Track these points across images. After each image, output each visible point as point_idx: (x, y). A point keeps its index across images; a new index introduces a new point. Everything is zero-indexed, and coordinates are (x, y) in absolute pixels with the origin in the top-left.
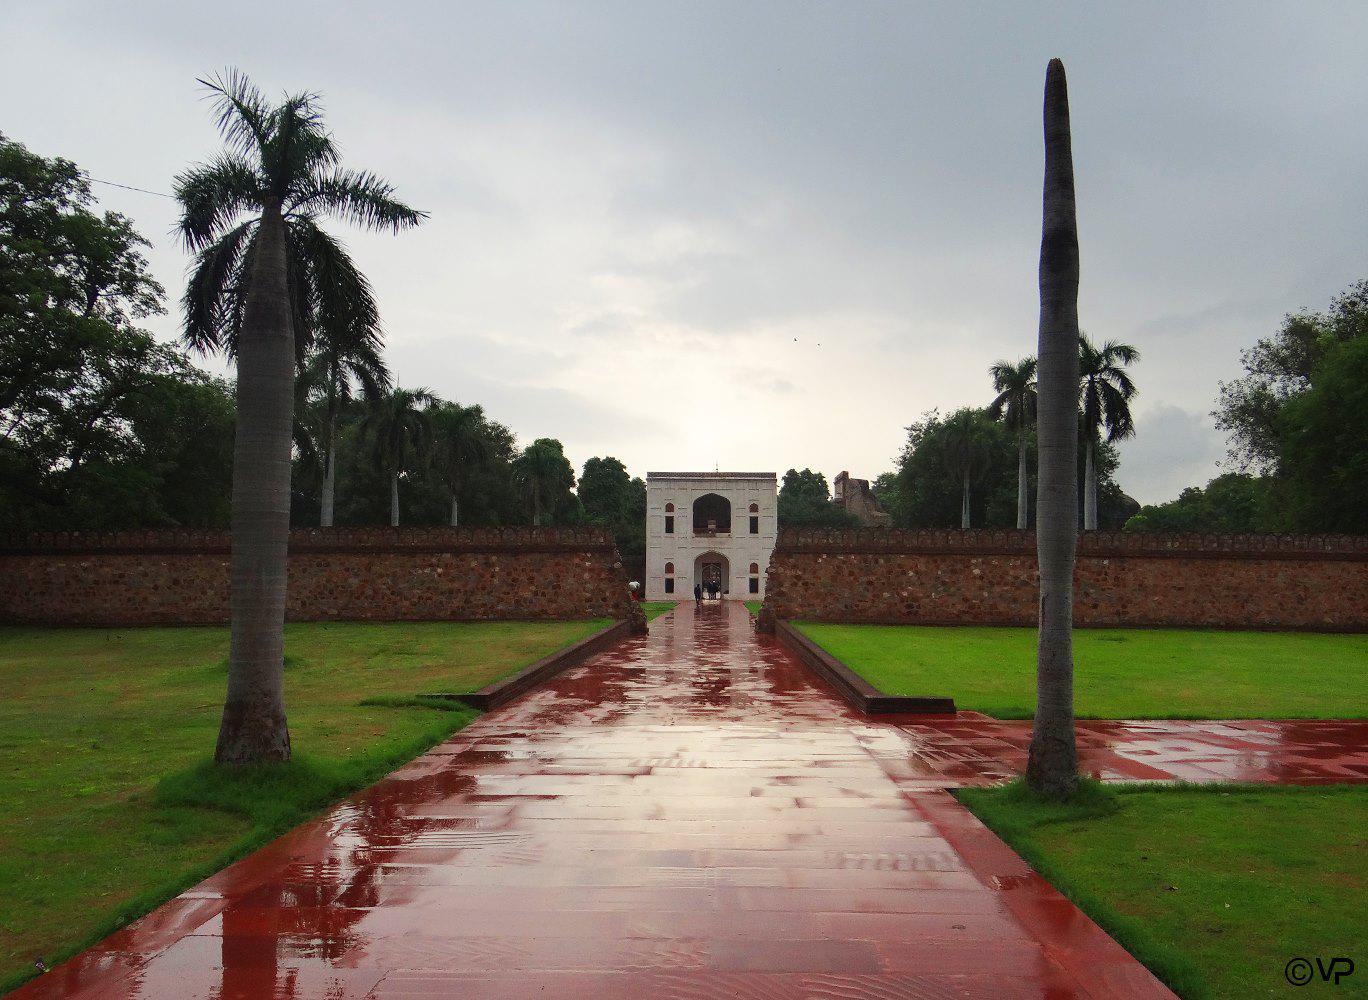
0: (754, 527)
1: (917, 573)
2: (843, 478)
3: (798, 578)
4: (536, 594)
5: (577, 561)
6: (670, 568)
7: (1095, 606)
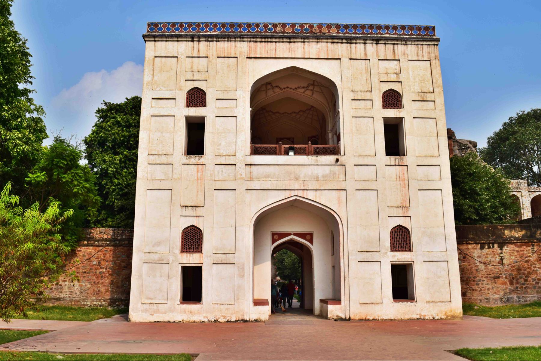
0: (394, 139)
6: (192, 239)
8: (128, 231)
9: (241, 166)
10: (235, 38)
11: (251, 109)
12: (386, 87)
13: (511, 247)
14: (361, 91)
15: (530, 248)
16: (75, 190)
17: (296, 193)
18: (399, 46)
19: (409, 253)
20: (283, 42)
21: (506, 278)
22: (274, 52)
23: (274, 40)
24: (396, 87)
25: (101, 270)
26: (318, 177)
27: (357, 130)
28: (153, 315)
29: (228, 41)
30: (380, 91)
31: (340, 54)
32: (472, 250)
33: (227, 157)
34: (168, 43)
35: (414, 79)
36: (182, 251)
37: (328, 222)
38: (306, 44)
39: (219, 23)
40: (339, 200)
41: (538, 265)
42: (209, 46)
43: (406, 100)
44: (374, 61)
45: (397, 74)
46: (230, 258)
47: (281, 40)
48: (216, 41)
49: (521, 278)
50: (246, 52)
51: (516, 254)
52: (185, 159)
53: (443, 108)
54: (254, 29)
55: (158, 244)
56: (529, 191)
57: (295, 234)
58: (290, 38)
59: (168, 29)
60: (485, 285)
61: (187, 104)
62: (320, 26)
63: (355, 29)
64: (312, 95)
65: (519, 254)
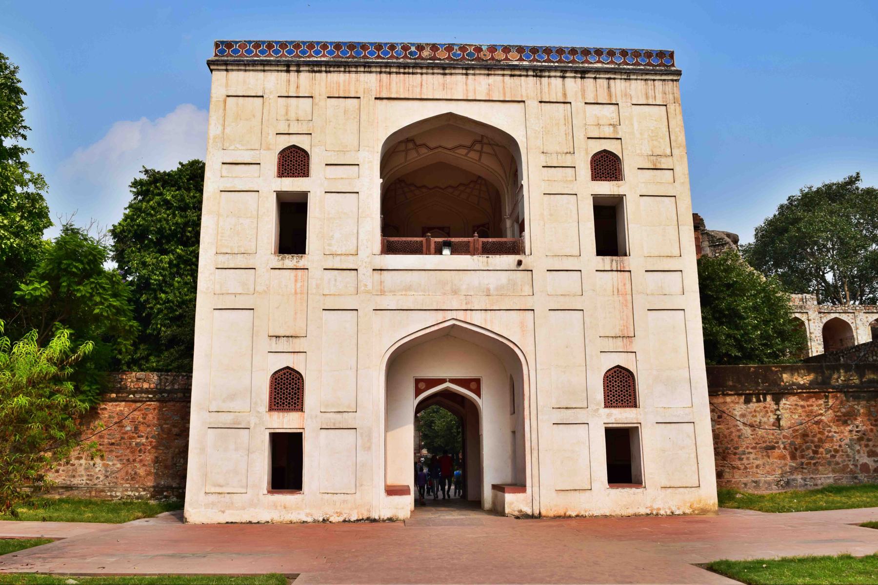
6: (287, 389)
8: (183, 376)
9: (365, 272)
10: (356, 66)
11: (381, 181)
12: (597, 147)
13: (793, 399)
14: (557, 153)
15: (821, 402)
16: (97, 311)
17: (454, 315)
18: (618, 81)
19: (633, 409)
20: (433, 74)
21: (785, 448)
22: (418, 90)
23: (419, 71)
24: (612, 147)
25: (138, 440)
26: (488, 290)
27: (551, 215)
28: (223, 512)
29: (345, 72)
30: (587, 153)
31: (524, 94)
32: (732, 405)
33: (343, 257)
34: (247, 73)
35: (641, 134)
36: (271, 409)
37: (505, 361)
38: (470, 77)
39: (331, 43)
40: (522, 325)
41: (834, 428)
42: (313, 79)
43: (628, 167)
44: (578, 104)
45: (614, 126)
46: (348, 420)
47: (430, 71)
48: (326, 72)
49: (808, 448)
50: (373, 89)
51: (800, 410)
52: (276, 261)
53: (687, 180)
54: (386, 53)
55: (232, 397)
56: (820, 313)
57: (452, 381)
58: (444, 68)
59: (249, 52)
60: (752, 461)
61: (279, 172)
62: (492, 49)
63: (548, 54)
64: (480, 159)
65: (805, 411)
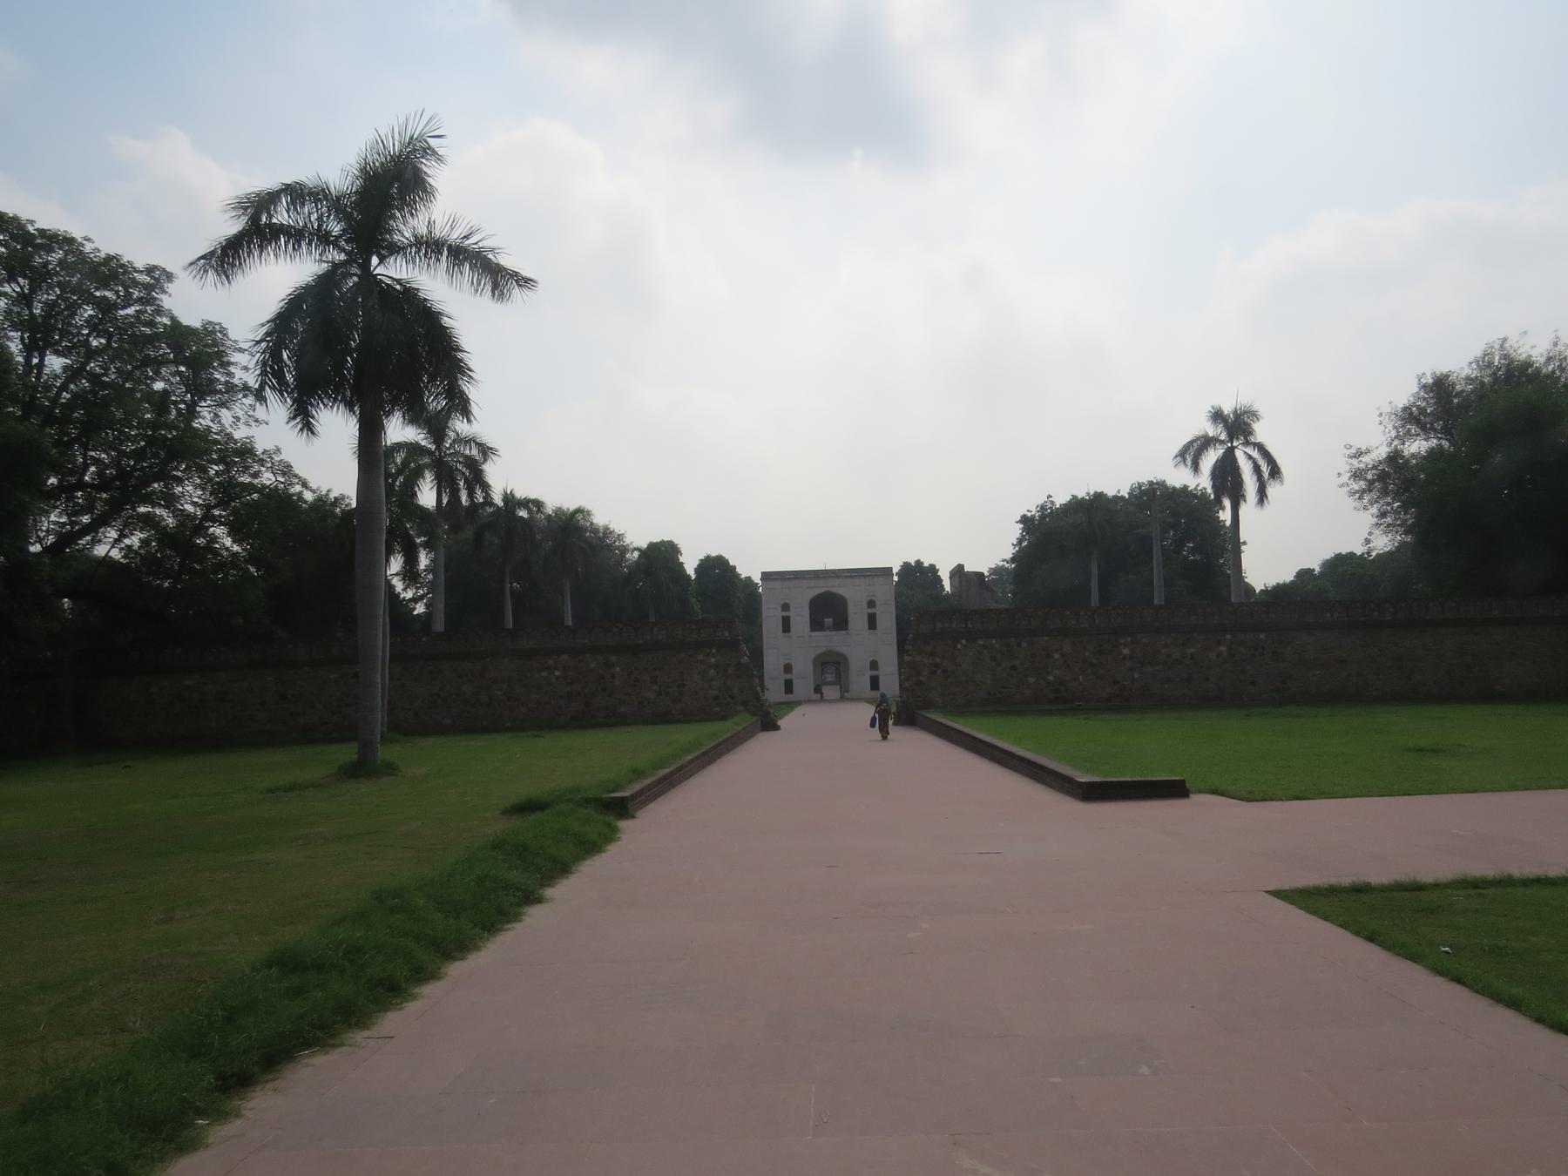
0: (872, 622)
1: (1062, 655)
2: (958, 572)
3: (937, 665)
4: (660, 693)
5: (700, 657)
6: (788, 668)
7: (1253, 683)
